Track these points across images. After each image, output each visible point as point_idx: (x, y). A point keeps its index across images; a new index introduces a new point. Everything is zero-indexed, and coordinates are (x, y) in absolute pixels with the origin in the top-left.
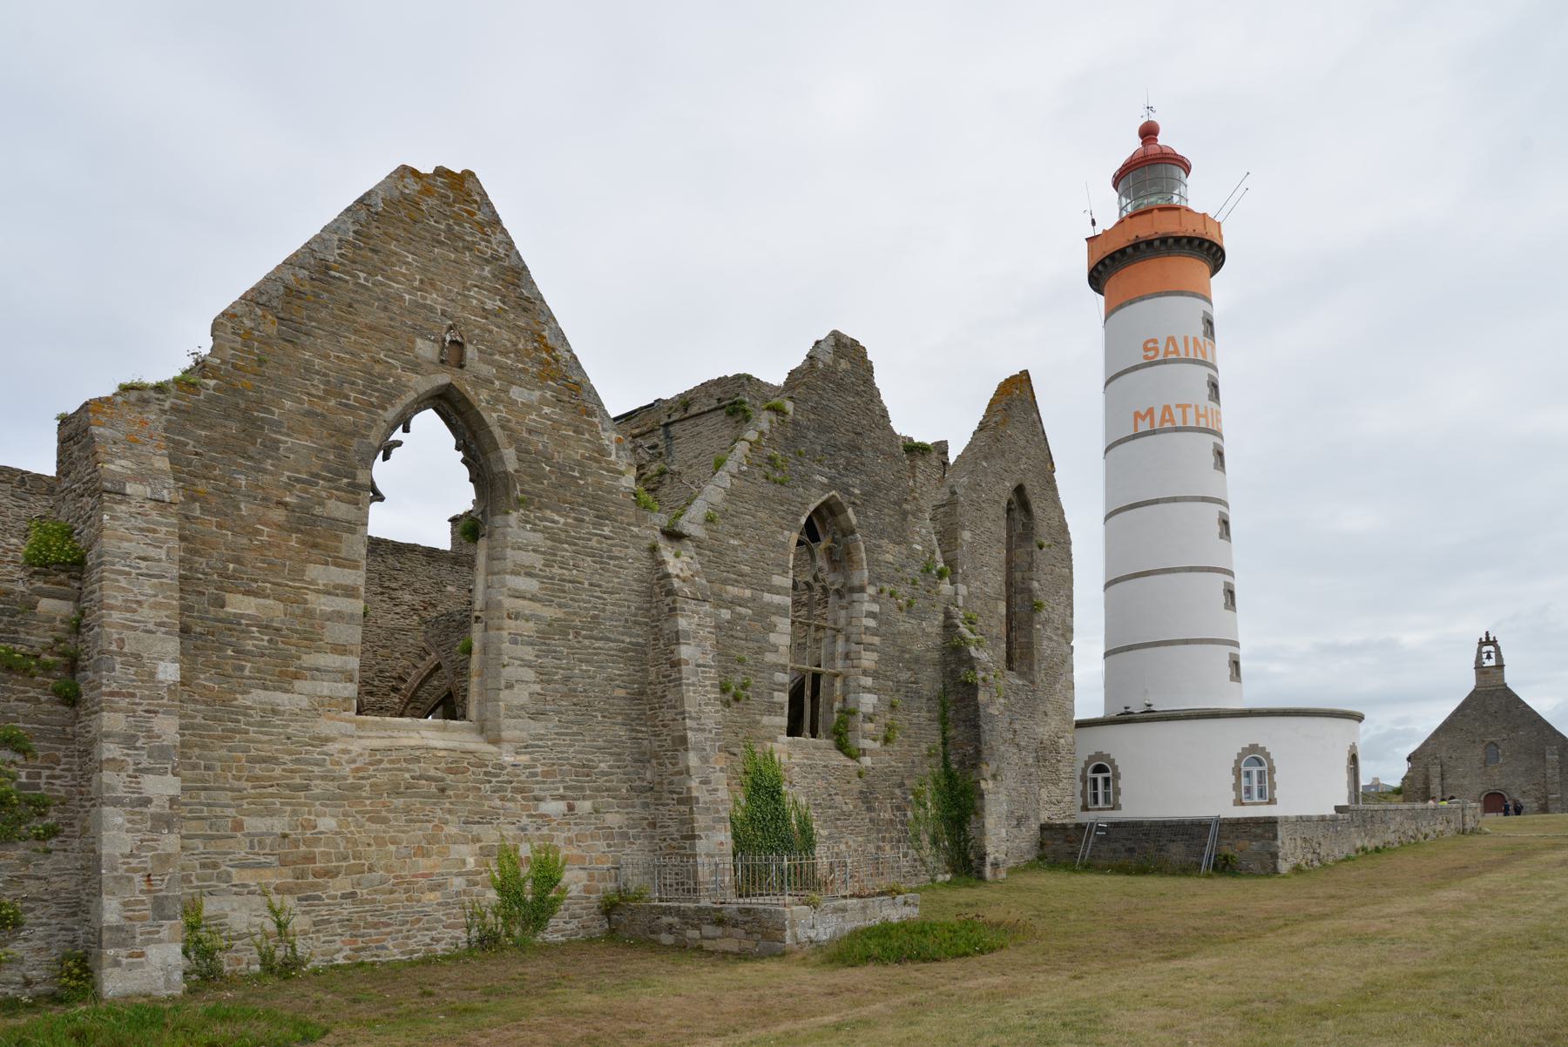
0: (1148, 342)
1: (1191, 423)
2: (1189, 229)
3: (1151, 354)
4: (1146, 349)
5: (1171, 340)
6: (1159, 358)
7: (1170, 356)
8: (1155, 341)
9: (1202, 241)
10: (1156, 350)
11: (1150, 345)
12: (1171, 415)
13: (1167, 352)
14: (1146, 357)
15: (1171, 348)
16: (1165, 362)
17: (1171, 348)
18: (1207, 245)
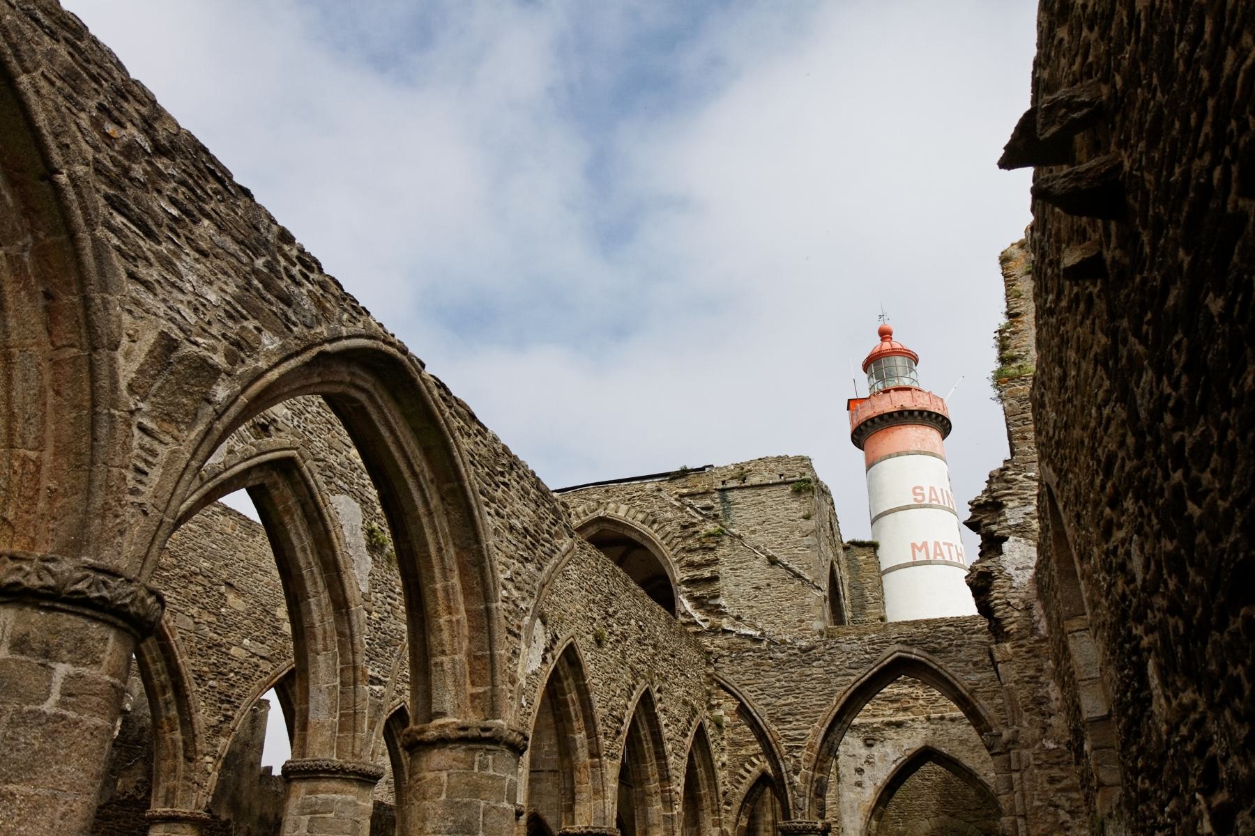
0: (915, 488)
1: (955, 560)
2: (922, 403)
3: (920, 498)
4: (915, 494)
5: (932, 489)
6: (926, 502)
7: (934, 503)
8: (922, 489)
9: (938, 415)
10: (923, 495)
11: (918, 491)
12: (941, 550)
13: (931, 500)
14: (915, 500)
15: (934, 497)
16: (930, 506)
17: (934, 497)
18: (940, 419)
